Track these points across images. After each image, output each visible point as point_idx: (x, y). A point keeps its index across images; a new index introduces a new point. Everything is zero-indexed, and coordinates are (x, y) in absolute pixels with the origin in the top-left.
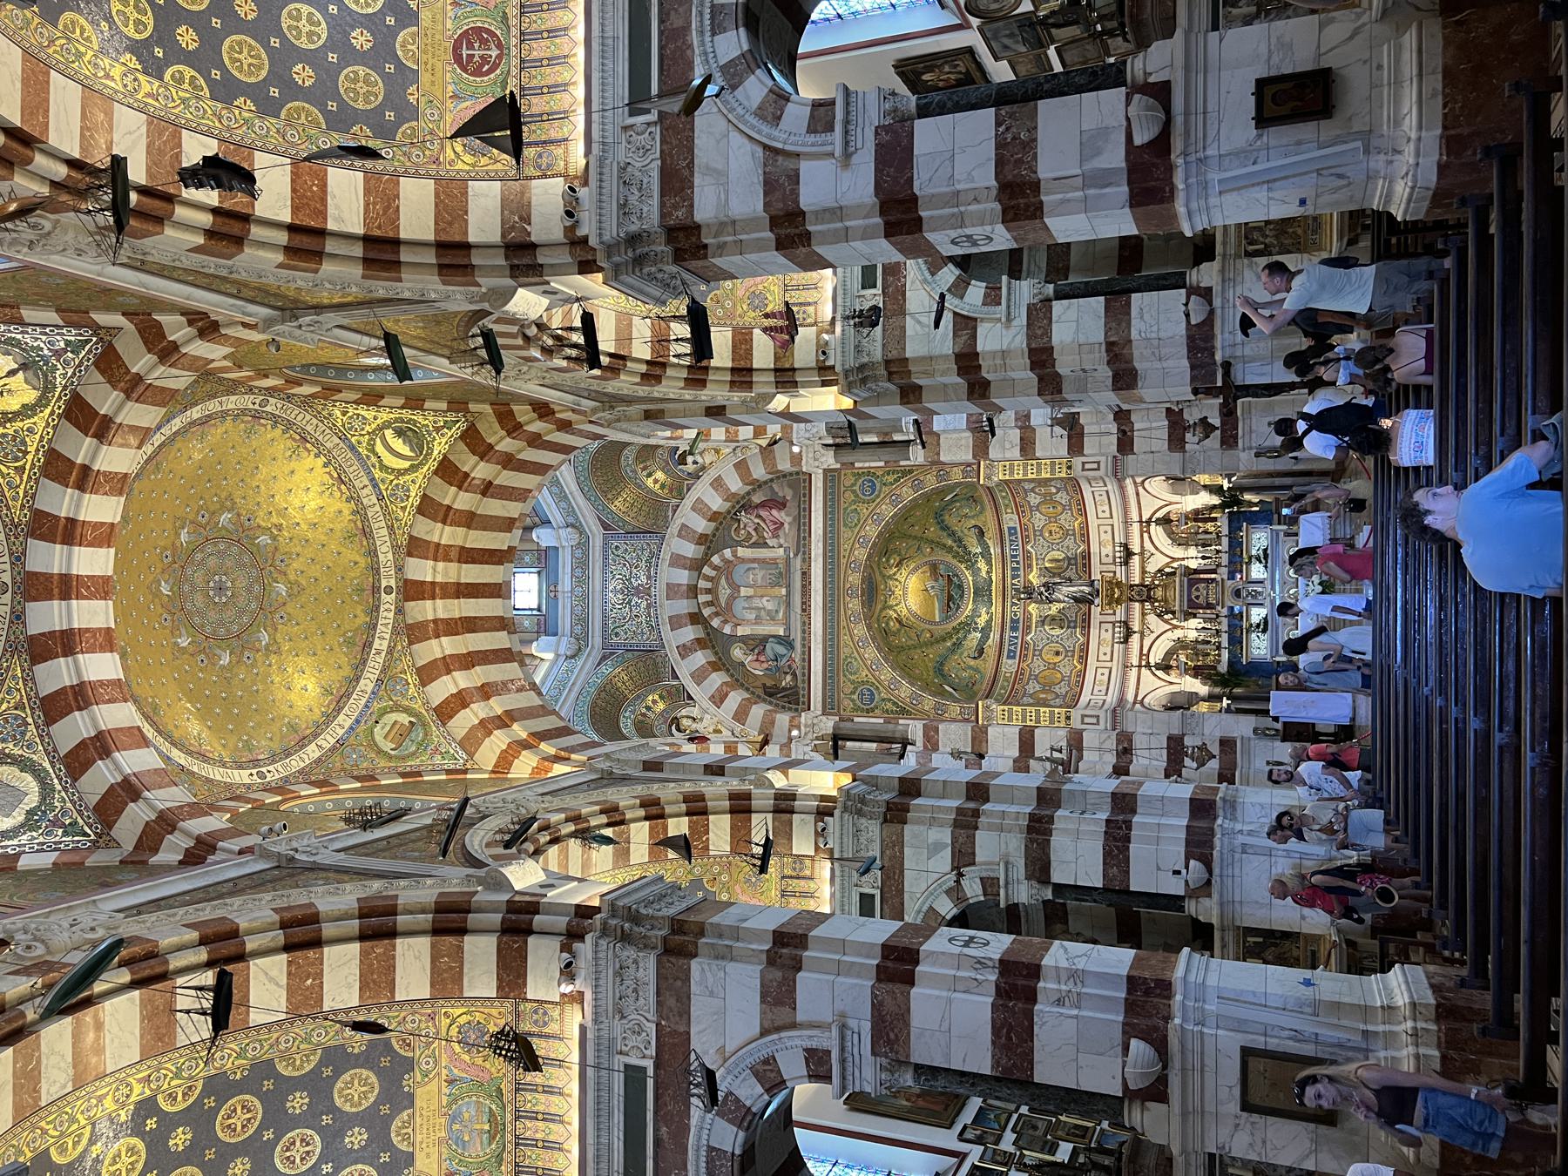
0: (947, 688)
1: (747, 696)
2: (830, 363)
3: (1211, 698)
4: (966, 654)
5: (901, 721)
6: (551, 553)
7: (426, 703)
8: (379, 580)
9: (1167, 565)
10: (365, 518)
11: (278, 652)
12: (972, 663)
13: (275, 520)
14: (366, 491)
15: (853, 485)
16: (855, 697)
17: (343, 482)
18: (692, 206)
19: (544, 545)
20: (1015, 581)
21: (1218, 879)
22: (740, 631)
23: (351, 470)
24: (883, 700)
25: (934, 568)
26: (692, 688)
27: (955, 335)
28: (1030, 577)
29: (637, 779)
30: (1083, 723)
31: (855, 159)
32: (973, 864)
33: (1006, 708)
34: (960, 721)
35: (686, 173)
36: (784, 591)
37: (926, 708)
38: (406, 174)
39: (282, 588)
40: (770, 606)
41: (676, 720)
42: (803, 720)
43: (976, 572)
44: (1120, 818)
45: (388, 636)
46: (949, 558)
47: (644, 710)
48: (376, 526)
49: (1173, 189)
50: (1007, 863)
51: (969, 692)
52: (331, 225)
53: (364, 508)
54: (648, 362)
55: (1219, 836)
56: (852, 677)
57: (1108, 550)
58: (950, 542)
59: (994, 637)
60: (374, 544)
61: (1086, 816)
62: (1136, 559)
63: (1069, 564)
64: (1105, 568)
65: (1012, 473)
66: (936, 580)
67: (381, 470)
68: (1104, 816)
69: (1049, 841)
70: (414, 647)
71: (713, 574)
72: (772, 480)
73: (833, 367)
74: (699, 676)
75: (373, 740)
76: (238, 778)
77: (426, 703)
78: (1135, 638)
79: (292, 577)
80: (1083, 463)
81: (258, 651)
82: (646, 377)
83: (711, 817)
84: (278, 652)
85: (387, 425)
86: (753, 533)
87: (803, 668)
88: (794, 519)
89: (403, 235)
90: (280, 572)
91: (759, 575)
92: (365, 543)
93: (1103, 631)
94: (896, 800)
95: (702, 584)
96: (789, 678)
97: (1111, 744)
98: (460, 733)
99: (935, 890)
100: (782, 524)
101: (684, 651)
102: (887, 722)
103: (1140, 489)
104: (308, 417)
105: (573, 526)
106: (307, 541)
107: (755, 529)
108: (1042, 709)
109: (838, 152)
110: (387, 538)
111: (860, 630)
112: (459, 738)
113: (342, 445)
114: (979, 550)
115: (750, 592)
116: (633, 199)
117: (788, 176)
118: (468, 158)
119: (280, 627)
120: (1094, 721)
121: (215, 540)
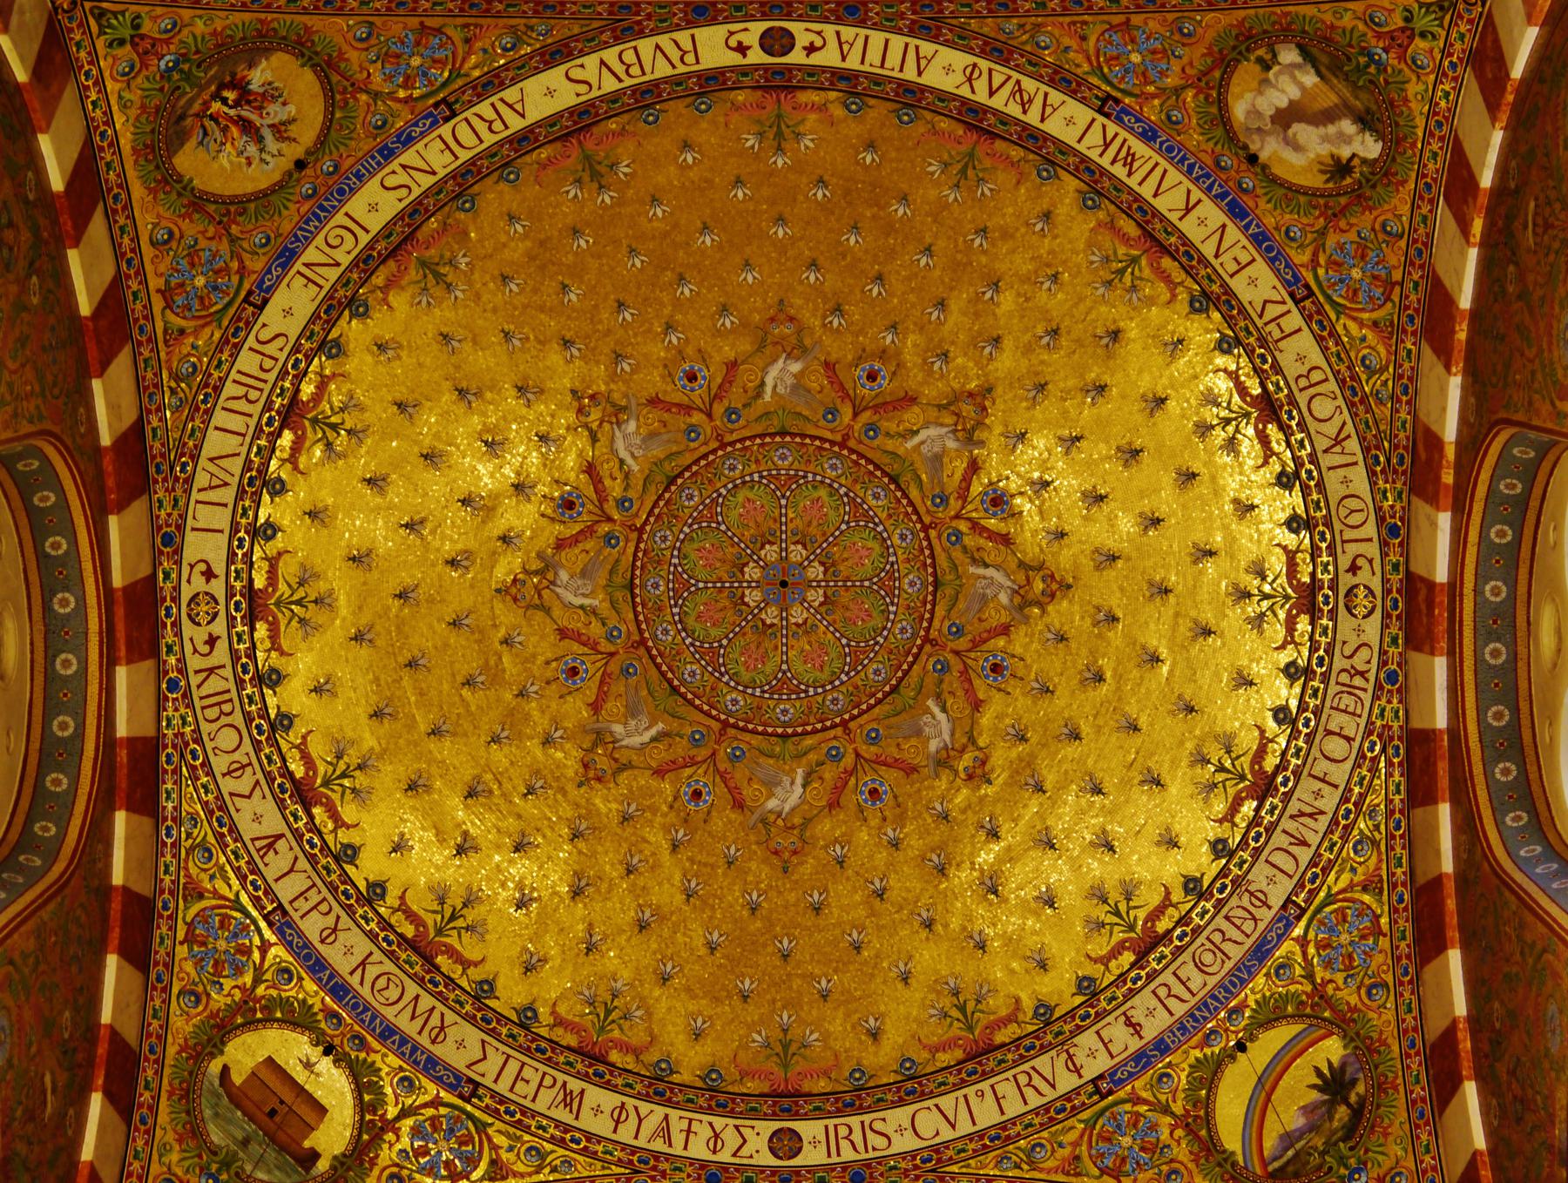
8: (819, 1114)
10: (1026, 1048)
11: (590, 774)
13: (1002, 757)
14: (1118, 1033)
23: (1189, 971)
39: (789, 796)
45: (625, 1134)
48: (1006, 1088)
53: (1063, 1042)
60: (944, 1089)
75: (269, 1020)
76: (204, 516)
79: (825, 827)
81: (596, 707)
84: (590, 774)
90: (839, 789)
92: (944, 1058)
106: (942, 871)
110: (964, 1127)
113: (1266, 916)
119: (667, 787)
121: (926, 559)
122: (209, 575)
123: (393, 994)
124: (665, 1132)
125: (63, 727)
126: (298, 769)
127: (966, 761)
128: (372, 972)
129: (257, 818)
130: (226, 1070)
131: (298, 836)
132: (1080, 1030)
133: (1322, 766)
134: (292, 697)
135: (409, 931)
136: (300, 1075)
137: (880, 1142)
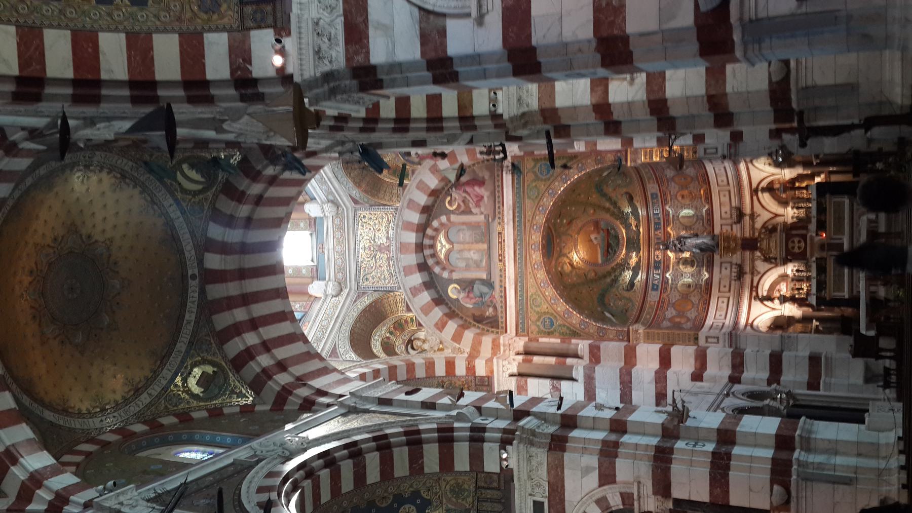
0: (607, 314)
1: (461, 322)
2: (500, 111)
3: (806, 319)
4: (621, 287)
5: (573, 341)
6: (318, 221)
7: (224, 357)
9: (772, 218)
12: (626, 294)
15: (535, 166)
16: (539, 323)
17: (154, 203)
18: (368, 52)
19: (313, 215)
20: (657, 232)
21: (795, 500)
22: (455, 276)
23: (160, 194)
24: (560, 325)
25: (596, 224)
26: (422, 319)
27: (592, 89)
28: (669, 229)
29: (374, 412)
30: (707, 341)
31: (487, 19)
32: (614, 482)
33: (649, 331)
34: (616, 341)
35: (362, 26)
36: (485, 246)
37: (592, 331)
38: (158, 31)
40: (475, 256)
41: (410, 342)
42: (502, 341)
43: (628, 226)
44: (723, 449)
45: (195, 310)
46: (607, 216)
47: (388, 335)
49: (733, 41)
50: (639, 483)
51: (624, 317)
52: (104, 76)
53: (172, 220)
54: (365, 120)
55: (795, 467)
56: (537, 309)
57: (727, 208)
58: (607, 205)
59: (641, 277)
61: (698, 448)
62: (747, 218)
63: (697, 219)
64: (724, 222)
65: (651, 157)
66: (598, 233)
67: (182, 192)
68: (710, 447)
69: (669, 468)
70: (214, 317)
71: (434, 233)
72: (474, 165)
73: (502, 115)
74: (426, 310)
77: (224, 357)
78: (747, 278)
80: (705, 150)
82: (362, 130)
83: (425, 446)
85: (184, 160)
86: (462, 204)
87: (501, 302)
88: (491, 193)
89: (158, 77)
91: (466, 235)
93: (723, 269)
94: (559, 433)
95: (427, 242)
96: (491, 310)
97: (728, 361)
98: (250, 377)
99: (587, 500)
100: (482, 197)
101: (415, 291)
102: (563, 341)
103: (750, 166)
104: (125, 161)
105: (332, 202)
106: (132, 247)
107: (463, 201)
108: (677, 332)
109: (474, 14)
110: (190, 240)
111: (542, 275)
112: (249, 381)
114: (629, 210)
115: (462, 246)
116: (324, 47)
117: (439, 32)
118: (205, 17)
120: (716, 340)
122: (102, 421)
123: (174, 363)
124: (193, 302)
125: (157, 440)
126: (132, 393)
127: (108, 242)
128: (170, 368)
129: (145, 398)
130: (201, 392)
131: (146, 389)
132: (170, 216)
133: (123, 164)
134: (118, 397)
135: (159, 362)
136: (198, 377)
137: (193, 258)
